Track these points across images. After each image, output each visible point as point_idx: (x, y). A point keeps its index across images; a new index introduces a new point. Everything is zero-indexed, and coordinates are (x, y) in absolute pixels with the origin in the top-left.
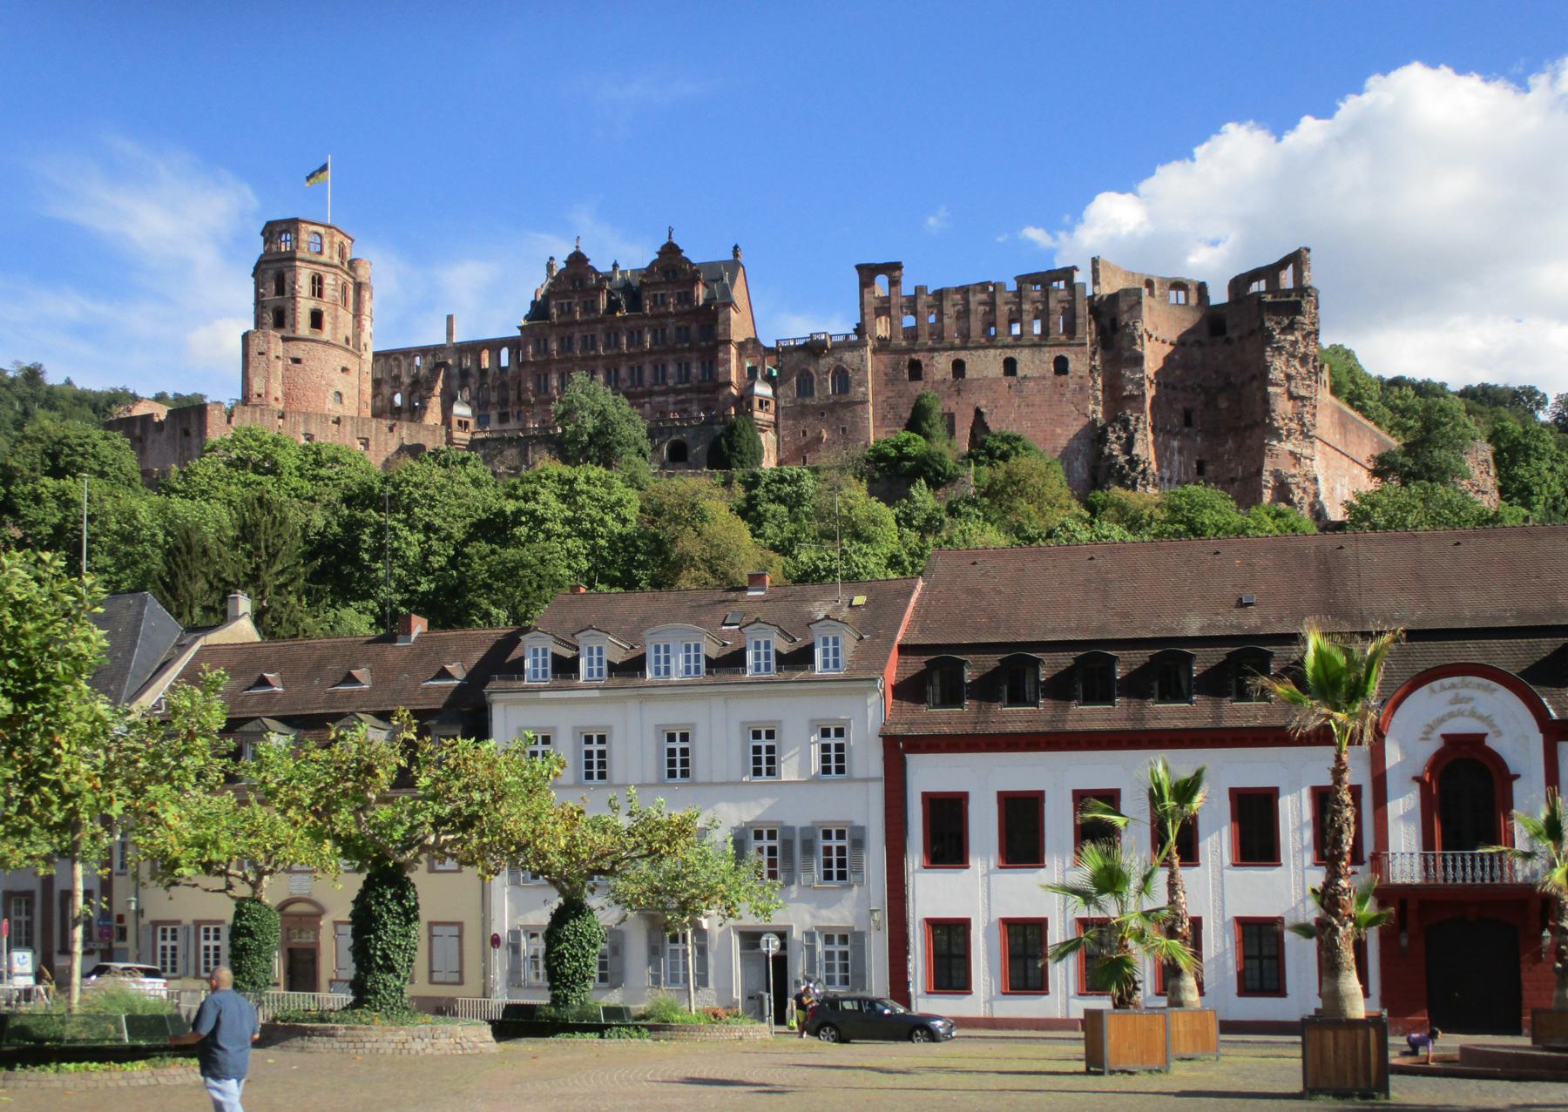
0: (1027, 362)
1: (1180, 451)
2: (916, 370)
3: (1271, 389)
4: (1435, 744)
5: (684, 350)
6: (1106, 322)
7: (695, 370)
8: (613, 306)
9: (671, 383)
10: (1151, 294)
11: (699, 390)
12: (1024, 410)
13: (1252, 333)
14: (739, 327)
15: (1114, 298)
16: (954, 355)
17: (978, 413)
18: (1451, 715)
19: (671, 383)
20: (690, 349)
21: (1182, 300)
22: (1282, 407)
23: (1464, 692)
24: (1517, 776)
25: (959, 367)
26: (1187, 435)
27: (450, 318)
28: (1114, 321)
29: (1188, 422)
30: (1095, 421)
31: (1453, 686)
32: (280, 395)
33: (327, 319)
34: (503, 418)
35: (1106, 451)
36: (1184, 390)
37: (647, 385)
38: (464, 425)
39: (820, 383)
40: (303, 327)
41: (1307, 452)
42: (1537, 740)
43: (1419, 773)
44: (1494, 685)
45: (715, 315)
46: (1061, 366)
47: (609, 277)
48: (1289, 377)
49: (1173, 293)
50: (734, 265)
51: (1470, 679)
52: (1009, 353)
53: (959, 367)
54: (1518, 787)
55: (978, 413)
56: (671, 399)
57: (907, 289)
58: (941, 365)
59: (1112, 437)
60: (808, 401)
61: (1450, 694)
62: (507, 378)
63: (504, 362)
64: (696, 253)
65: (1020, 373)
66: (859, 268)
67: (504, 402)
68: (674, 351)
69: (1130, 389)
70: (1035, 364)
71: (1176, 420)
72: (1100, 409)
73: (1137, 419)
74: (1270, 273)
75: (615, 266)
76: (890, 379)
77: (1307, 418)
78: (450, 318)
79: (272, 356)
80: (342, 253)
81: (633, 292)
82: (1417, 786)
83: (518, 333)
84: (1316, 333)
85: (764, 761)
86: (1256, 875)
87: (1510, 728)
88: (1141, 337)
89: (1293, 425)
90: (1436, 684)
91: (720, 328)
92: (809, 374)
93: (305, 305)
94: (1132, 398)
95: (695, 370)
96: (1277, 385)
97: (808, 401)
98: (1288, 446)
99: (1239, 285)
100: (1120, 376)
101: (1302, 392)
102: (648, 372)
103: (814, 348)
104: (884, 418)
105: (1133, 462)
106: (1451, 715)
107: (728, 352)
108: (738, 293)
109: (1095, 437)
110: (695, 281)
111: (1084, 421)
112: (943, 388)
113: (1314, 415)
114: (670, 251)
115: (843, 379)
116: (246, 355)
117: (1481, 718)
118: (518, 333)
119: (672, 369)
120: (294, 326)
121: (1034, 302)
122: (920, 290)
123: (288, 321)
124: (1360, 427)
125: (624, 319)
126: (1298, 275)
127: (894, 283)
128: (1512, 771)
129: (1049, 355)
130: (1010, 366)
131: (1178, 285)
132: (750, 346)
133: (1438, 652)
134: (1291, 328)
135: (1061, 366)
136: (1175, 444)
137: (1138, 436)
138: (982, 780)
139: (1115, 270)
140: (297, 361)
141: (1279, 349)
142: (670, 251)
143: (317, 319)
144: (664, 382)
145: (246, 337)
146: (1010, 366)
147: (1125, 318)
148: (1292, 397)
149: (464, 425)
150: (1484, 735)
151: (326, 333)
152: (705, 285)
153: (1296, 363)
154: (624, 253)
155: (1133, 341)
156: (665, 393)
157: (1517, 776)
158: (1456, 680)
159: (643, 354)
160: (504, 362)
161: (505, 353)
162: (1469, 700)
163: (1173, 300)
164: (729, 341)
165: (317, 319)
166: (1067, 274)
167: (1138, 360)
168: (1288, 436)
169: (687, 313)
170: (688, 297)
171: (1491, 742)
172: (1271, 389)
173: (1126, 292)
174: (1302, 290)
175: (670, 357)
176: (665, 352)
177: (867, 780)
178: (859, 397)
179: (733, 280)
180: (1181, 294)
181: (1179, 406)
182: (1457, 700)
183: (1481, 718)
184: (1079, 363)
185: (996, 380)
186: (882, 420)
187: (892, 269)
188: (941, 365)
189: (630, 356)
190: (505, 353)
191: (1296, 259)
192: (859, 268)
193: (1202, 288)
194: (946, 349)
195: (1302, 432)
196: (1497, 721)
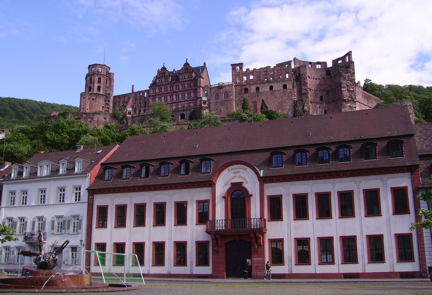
0: (277, 87)
1: (319, 108)
2: (246, 90)
3: (342, 89)
4: (229, 186)
5: (189, 90)
6: (297, 74)
7: (192, 95)
8: (172, 80)
9: (186, 99)
10: (311, 67)
11: (193, 100)
12: (275, 99)
13: (337, 74)
14: (203, 83)
15: (299, 68)
16: (256, 86)
17: (263, 100)
18: (233, 177)
19: (186, 99)
20: (191, 90)
21: (320, 67)
22: (346, 94)
23: (238, 170)
24: (251, 195)
25: (258, 89)
26: (321, 103)
27: (133, 86)
28: (299, 74)
29: (321, 99)
30: (294, 101)
31: (234, 169)
32: (88, 108)
33: (101, 89)
34: (145, 110)
35: (297, 109)
36: (320, 91)
37: (180, 99)
38: (130, 113)
39: (221, 96)
40: (96, 91)
41: (354, 106)
42: (258, 183)
43: (224, 195)
44: (246, 167)
45: (197, 79)
46: (285, 87)
47: (172, 72)
48: (347, 85)
49: (317, 66)
50: (204, 68)
51: (239, 165)
52: (271, 84)
53: (258, 89)
54: (252, 199)
55: (263, 100)
56: (186, 103)
57: (244, 70)
58: (253, 89)
59: (298, 105)
60: (218, 101)
61: (233, 171)
62: (146, 100)
63: (146, 96)
64: (193, 65)
65: (274, 90)
66: (231, 65)
67: (145, 106)
68: (187, 90)
69: (304, 91)
70: (277, 87)
71: (318, 100)
72: (296, 97)
73: (306, 100)
74: (343, 58)
75: (174, 70)
76: (239, 94)
77: (353, 97)
78: (133, 86)
79: (87, 98)
80: (107, 72)
81: (176, 76)
82: (224, 200)
83: (148, 89)
84: (354, 73)
85: (62, 198)
86: (372, 220)
87: (249, 180)
88: (306, 77)
89: (349, 99)
90: (230, 168)
91: (198, 84)
92: (218, 94)
93: (96, 85)
94: (305, 94)
95: (192, 95)
96: (344, 88)
97: (218, 101)
98: (349, 104)
99: (335, 62)
100: (301, 88)
101: (351, 89)
102: (180, 96)
103: (220, 87)
104: (238, 104)
105: (304, 111)
106: (233, 177)
107: (200, 89)
108: (203, 75)
109: (295, 105)
110: (193, 72)
111: (291, 102)
112: (253, 95)
113: (355, 95)
114: (187, 64)
115: (227, 94)
116: (81, 99)
117: (242, 178)
118: (148, 89)
119: (186, 95)
120: (93, 91)
121: (277, 70)
122: (248, 70)
123: (92, 90)
124: (371, 98)
125: (174, 83)
126: (350, 58)
127: (241, 68)
128: (250, 193)
129: (281, 84)
130: (271, 88)
131: (319, 63)
132: (206, 88)
133: (234, 158)
134: (347, 73)
135: (285, 87)
136: (318, 106)
137: (305, 104)
138: (111, 201)
139: (300, 61)
140: (93, 99)
141: (345, 79)
142: (187, 64)
143: (99, 88)
144: (184, 99)
145: (81, 94)
146: (271, 88)
147: (302, 73)
148: (349, 91)
149: (130, 113)
150: (242, 183)
151: (101, 92)
152: (195, 73)
153: (349, 82)
154: (175, 65)
155: (305, 79)
156: (185, 101)
157: (251, 195)
158: (235, 166)
159: (179, 92)
160: (146, 96)
161: (146, 93)
162: (238, 172)
163: (317, 67)
164: (201, 87)
165: (99, 88)
166: (289, 63)
167: (306, 84)
168: (348, 101)
169: (190, 80)
170: (190, 76)
171: (245, 185)
172: (342, 89)
173: (302, 66)
174: (351, 63)
175: (186, 92)
176: (184, 91)
177: (84, 203)
178: (231, 99)
179: (202, 72)
180: (320, 65)
181: (319, 96)
182: (235, 173)
183: (242, 178)
184: (289, 86)
185: (267, 92)
186: (237, 105)
187: (241, 65)
188: (253, 89)
189: (175, 92)
190: (146, 93)
191: (349, 54)
192: (231, 65)
193: (325, 63)
194: (254, 85)
195: (352, 101)
196: (247, 178)
